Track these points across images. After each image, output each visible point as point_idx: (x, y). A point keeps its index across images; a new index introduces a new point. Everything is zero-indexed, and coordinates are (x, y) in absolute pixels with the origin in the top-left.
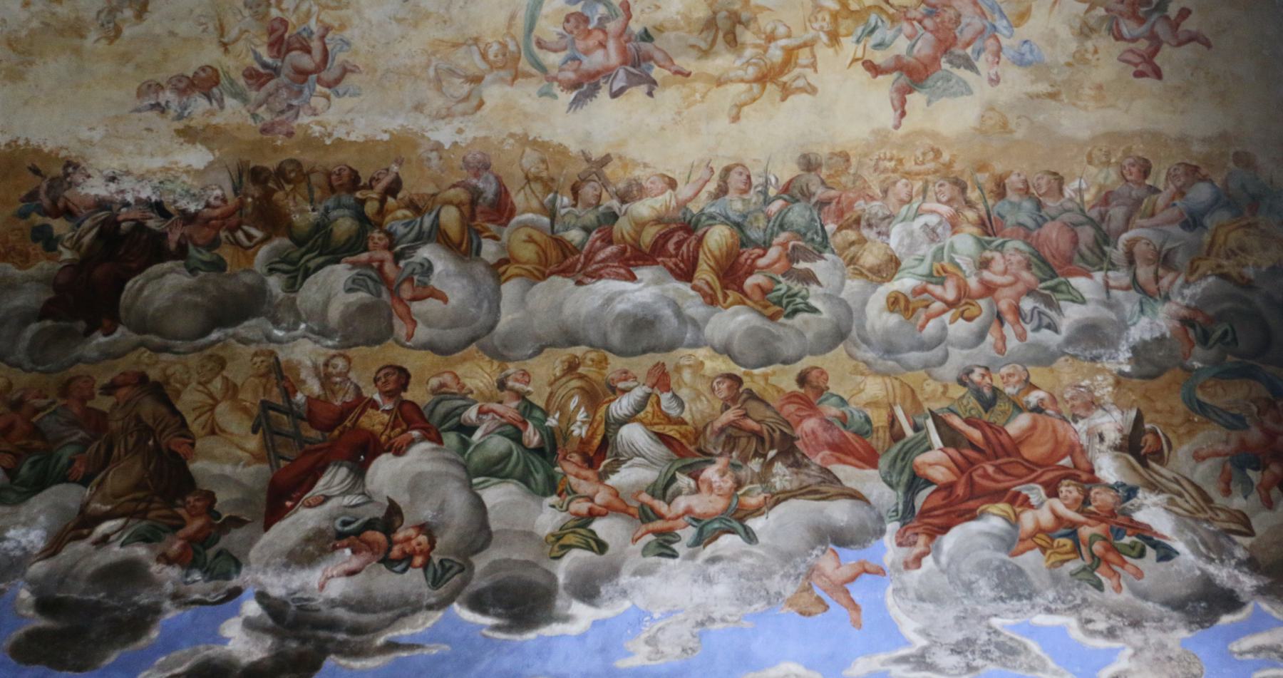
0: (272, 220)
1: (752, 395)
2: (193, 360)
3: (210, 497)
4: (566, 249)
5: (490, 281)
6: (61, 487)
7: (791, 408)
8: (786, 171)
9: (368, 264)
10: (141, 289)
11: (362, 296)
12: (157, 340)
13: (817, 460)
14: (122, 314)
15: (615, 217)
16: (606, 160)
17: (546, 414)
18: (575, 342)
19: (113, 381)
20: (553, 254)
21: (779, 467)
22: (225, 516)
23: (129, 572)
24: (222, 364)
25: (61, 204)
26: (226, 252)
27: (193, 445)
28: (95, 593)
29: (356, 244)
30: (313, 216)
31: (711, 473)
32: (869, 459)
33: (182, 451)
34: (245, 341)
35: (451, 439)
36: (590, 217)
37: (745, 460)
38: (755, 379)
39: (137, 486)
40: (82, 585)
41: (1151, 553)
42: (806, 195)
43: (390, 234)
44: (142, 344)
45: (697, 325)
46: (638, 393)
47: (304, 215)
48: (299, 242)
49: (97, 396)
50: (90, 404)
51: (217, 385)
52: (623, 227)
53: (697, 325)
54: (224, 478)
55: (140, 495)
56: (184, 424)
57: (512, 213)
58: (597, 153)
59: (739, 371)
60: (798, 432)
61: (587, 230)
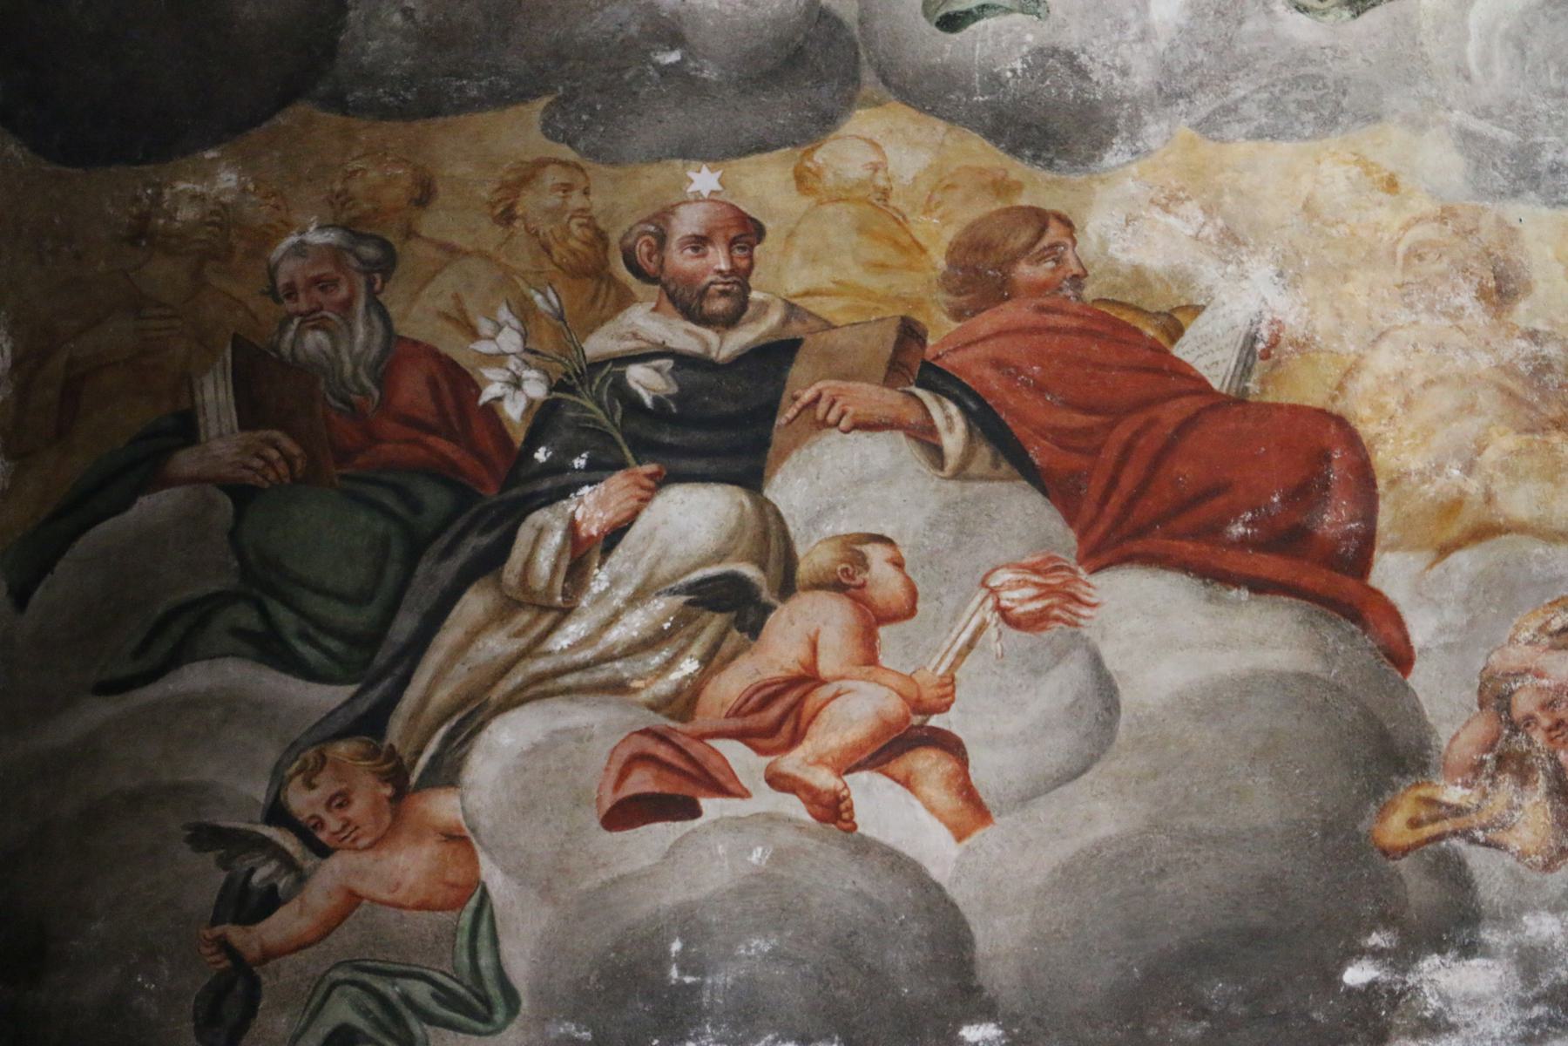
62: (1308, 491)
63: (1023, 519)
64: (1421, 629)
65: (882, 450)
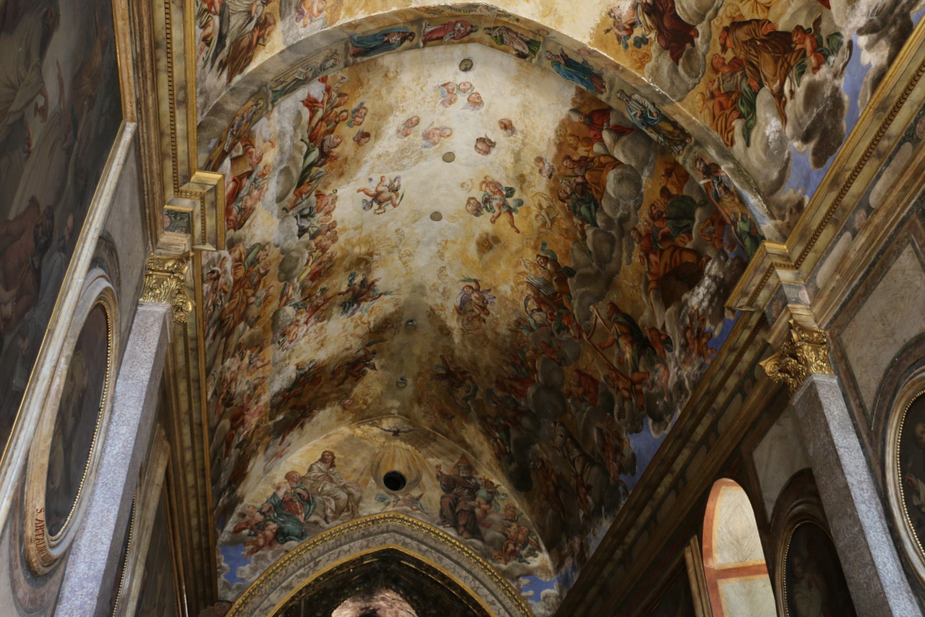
3: (799, 28)
6: (758, 97)
10: (683, 8)
12: (710, 13)
14: (691, 23)
19: (721, 45)
22: (811, 26)
23: (813, 91)
25: (628, 27)
27: (770, 22)
28: (812, 113)
33: (769, 30)
39: (776, 61)
40: (806, 116)
44: (710, 21)
49: (725, 56)
50: (727, 62)
54: (794, 15)
55: (780, 63)
56: (758, 21)
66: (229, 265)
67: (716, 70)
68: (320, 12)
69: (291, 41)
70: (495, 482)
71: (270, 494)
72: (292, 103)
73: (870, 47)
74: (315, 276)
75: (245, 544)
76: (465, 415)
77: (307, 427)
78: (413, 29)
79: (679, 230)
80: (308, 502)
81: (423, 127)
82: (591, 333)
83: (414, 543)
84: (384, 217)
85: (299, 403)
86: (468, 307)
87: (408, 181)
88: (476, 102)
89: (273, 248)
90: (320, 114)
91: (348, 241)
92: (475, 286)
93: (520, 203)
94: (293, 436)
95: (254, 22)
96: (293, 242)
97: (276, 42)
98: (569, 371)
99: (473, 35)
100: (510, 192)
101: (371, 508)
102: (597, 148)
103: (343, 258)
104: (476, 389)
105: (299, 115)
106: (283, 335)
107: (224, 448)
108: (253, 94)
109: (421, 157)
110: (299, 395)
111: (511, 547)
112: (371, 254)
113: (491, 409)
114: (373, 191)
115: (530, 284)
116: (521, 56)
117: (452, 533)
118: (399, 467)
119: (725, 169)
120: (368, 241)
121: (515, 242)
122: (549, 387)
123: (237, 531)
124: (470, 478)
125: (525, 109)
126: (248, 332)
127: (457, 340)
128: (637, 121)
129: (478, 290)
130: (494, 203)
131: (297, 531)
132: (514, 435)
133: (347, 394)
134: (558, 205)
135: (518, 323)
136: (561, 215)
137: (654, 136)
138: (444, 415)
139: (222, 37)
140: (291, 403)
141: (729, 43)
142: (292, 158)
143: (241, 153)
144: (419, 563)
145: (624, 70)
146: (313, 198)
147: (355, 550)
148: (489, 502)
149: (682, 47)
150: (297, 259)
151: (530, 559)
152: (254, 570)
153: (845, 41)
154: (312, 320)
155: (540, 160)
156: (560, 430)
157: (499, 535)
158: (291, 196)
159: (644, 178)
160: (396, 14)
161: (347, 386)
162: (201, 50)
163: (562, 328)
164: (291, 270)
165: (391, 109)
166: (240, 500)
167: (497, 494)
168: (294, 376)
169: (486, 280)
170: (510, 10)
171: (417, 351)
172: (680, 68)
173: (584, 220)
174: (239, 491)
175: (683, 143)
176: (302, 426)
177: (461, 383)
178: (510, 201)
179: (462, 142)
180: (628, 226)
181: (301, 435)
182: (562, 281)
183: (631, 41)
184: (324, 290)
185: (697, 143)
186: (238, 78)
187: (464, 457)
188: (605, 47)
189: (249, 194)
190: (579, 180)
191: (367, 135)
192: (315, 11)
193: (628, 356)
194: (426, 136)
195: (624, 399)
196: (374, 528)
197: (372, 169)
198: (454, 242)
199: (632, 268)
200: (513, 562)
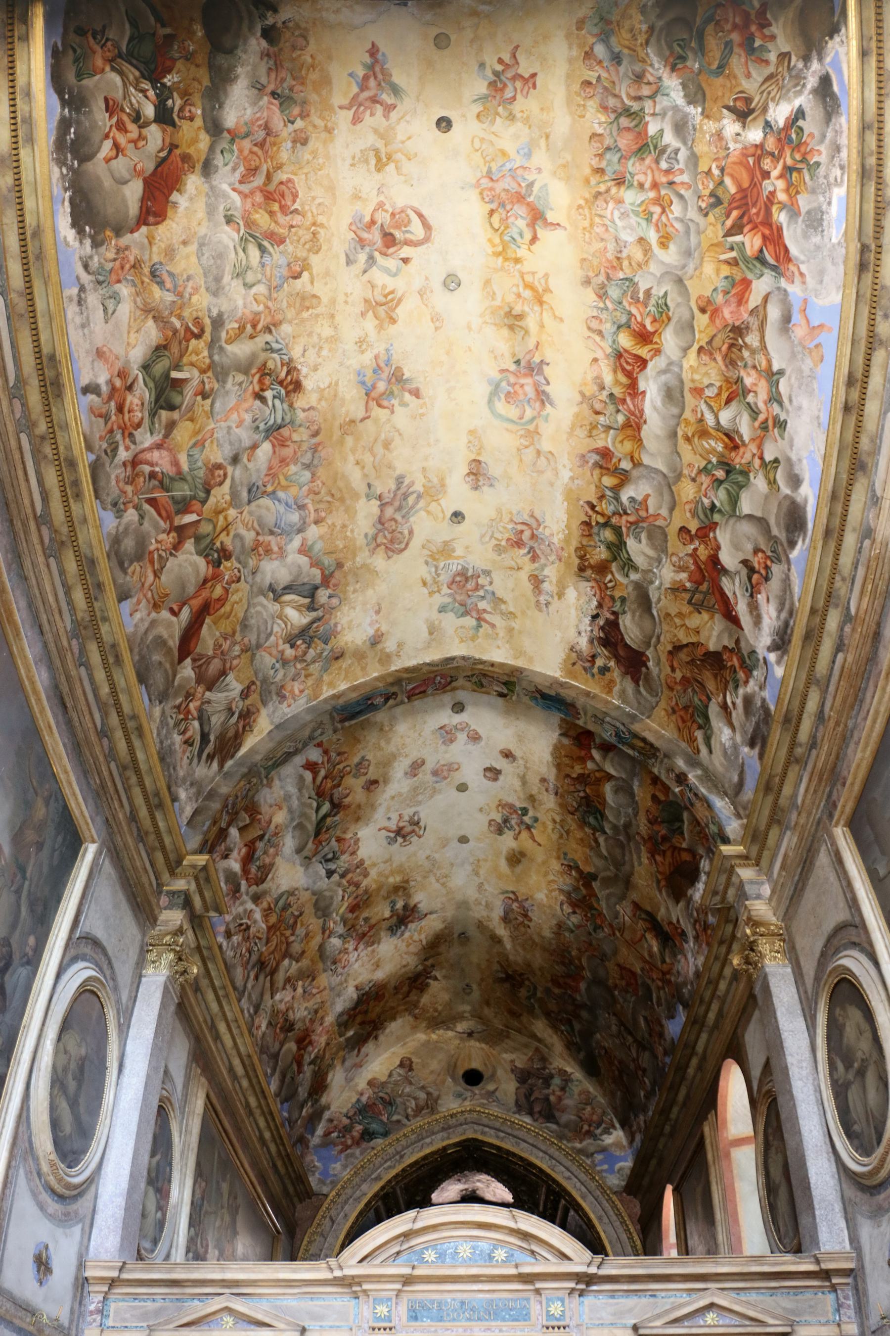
0: (602, 568)
1: (710, 343)
2: (665, 627)
4: (627, 425)
5: (641, 469)
7: (717, 321)
8: (590, 296)
9: (628, 529)
11: (643, 536)
13: (745, 316)
15: (611, 395)
16: (582, 393)
17: (710, 462)
18: (674, 435)
20: (629, 432)
21: (748, 340)
23: (748, 701)
24: (668, 615)
26: (617, 594)
29: (617, 530)
30: (603, 548)
31: (748, 381)
32: (746, 284)
34: (659, 600)
35: (717, 517)
36: (611, 408)
37: (742, 359)
38: (702, 338)
41: (800, 123)
42: (603, 286)
43: (614, 514)
45: (671, 363)
46: (704, 407)
47: (601, 553)
48: (615, 559)
51: (677, 621)
52: (618, 391)
53: (671, 363)
57: (607, 448)
58: (579, 398)
59: (696, 347)
60: (730, 322)
61: (618, 411)
62: (156, 215)
63: (150, 167)
64: (136, 235)
65: (159, 142)
66: (258, 916)
67: (671, 689)
68: (302, 691)
69: (277, 721)
70: (569, 1069)
71: (354, 1100)
72: (291, 770)
73: (779, 662)
74: (353, 909)
75: (335, 1145)
76: (531, 1011)
77: (382, 1038)
78: (395, 689)
79: (674, 831)
80: (390, 1104)
81: (430, 765)
82: (622, 930)
83: (492, 1132)
84: (411, 849)
85: (367, 1017)
86: (512, 916)
87: (426, 814)
88: (475, 738)
89: (303, 893)
90: (323, 773)
91: (380, 874)
92: (514, 897)
93: (536, 820)
94: (369, 1047)
95: (236, 716)
96: (323, 884)
97: (264, 725)
98: (611, 965)
99: (454, 684)
100: (525, 811)
101: (450, 1104)
102: (590, 765)
103: (379, 889)
104: (535, 988)
105: (301, 779)
106: (334, 963)
107: (295, 1067)
108: (244, 776)
109: (435, 791)
110: (366, 1012)
111: (586, 1127)
112: (407, 882)
113: (552, 1006)
114: (394, 828)
115: (561, 891)
116: (502, 695)
117: (528, 1119)
118: (475, 1065)
119: (693, 777)
120: (400, 870)
121: (540, 855)
122: (597, 981)
123: (327, 1134)
124: (544, 1068)
125: (520, 739)
126: (295, 966)
127: (509, 946)
128: (613, 740)
129: (516, 900)
130: (513, 822)
131: (382, 1130)
132: (577, 1026)
133: (416, 1005)
134: (569, 818)
135: (559, 926)
136: (574, 826)
137: (630, 752)
138: (513, 1014)
139: (205, 737)
140: (359, 1019)
141: (675, 664)
142: (303, 815)
143: (248, 821)
144: (499, 1148)
145: (595, 697)
146: (334, 843)
147: (437, 1143)
148: (563, 1089)
149: (640, 672)
150: (332, 898)
151: (604, 1137)
152: (345, 1167)
153: (761, 657)
154: (361, 946)
155: (543, 780)
156: (614, 1020)
157: (573, 1117)
158: (310, 845)
159: (635, 788)
160: (376, 679)
161: (413, 997)
162: (184, 752)
163: (597, 928)
164: (328, 907)
165: (394, 757)
166: (327, 1107)
167: (572, 1081)
168: (355, 996)
169: (522, 891)
170: (485, 658)
171: (475, 959)
172: (642, 689)
173: (595, 830)
174: (324, 1100)
175: (654, 755)
176: (376, 1038)
177: (521, 985)
178: (526, 819)
179: (471, 771)
180: (632, 831)
181: (377, 1046)
182: (588, 885)
183: (595, 670)
184: (366, 920)
185: (666, 756)
186: (230, 763)
187: (537, 1050)
188: (575, 678)
189: (265, 853)
190: (582, 794)
191: (376, 782)
192: (297, 692)
193: (655, 949)
194: (435, 773)
195: (659, 988)
196: (452, 1122)
197: (388, 809)
198: (486, 860)
199: (643, 869)
200: (588, 1141)
